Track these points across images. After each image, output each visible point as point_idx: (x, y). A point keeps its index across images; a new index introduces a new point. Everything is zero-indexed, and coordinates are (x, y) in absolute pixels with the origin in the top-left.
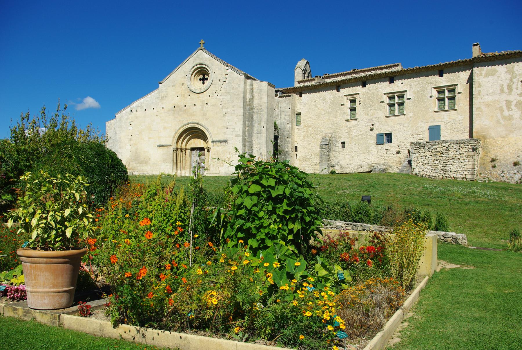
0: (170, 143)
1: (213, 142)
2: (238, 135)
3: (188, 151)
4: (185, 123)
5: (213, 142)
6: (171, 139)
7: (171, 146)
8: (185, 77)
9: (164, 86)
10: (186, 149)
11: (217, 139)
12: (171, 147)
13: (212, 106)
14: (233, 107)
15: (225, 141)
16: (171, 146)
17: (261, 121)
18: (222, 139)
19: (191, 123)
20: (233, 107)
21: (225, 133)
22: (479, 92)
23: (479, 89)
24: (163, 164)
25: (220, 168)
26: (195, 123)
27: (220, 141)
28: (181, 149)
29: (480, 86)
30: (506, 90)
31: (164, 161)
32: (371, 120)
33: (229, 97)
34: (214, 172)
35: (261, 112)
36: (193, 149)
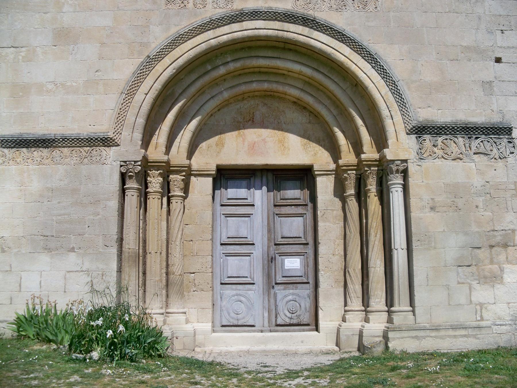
0: (103, 127)
1: (420, 130)
3: (202, 186)
5: (420, 130)
6: (112, 102)
7: (106, 142)
10: (189, 173)
12: (111, 155)
15: (500, 131)
16: (106, 142)
18: (479, 117)
19: (255, 15)
21: (488, 86)
24: (45, 258)
25: (482, 294)
27: (469, 130)
28: (167, 170)
31: (51, 240)
34: (441, 317)
36: (226, 176)
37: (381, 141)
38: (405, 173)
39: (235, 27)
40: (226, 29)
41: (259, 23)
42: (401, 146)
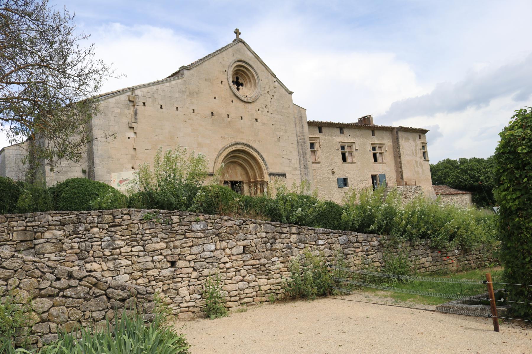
1: (270, 175)
2: (295, 169)
4: (231, 142)
5: (270, 175)
8: (223, 72)
9: (192, 75)
11: (274, 171)
13: (264, 124)
14: (286, 131)
15: (284, 175)
17: (306, 153)
18: (280, 171)
20: (286, 131)
22: (403, 152)
23: (403, 150)
26: (246, 145)
29: (403, 148)
30: (415, 154)
32: (331, 164)
33: (280, 117)
35: (304, 143)
37: (262, 175)
38: (267, 184)
39: (235, 146)
40: (234, 147)
41: (240, 146)
42: (267, 178)
